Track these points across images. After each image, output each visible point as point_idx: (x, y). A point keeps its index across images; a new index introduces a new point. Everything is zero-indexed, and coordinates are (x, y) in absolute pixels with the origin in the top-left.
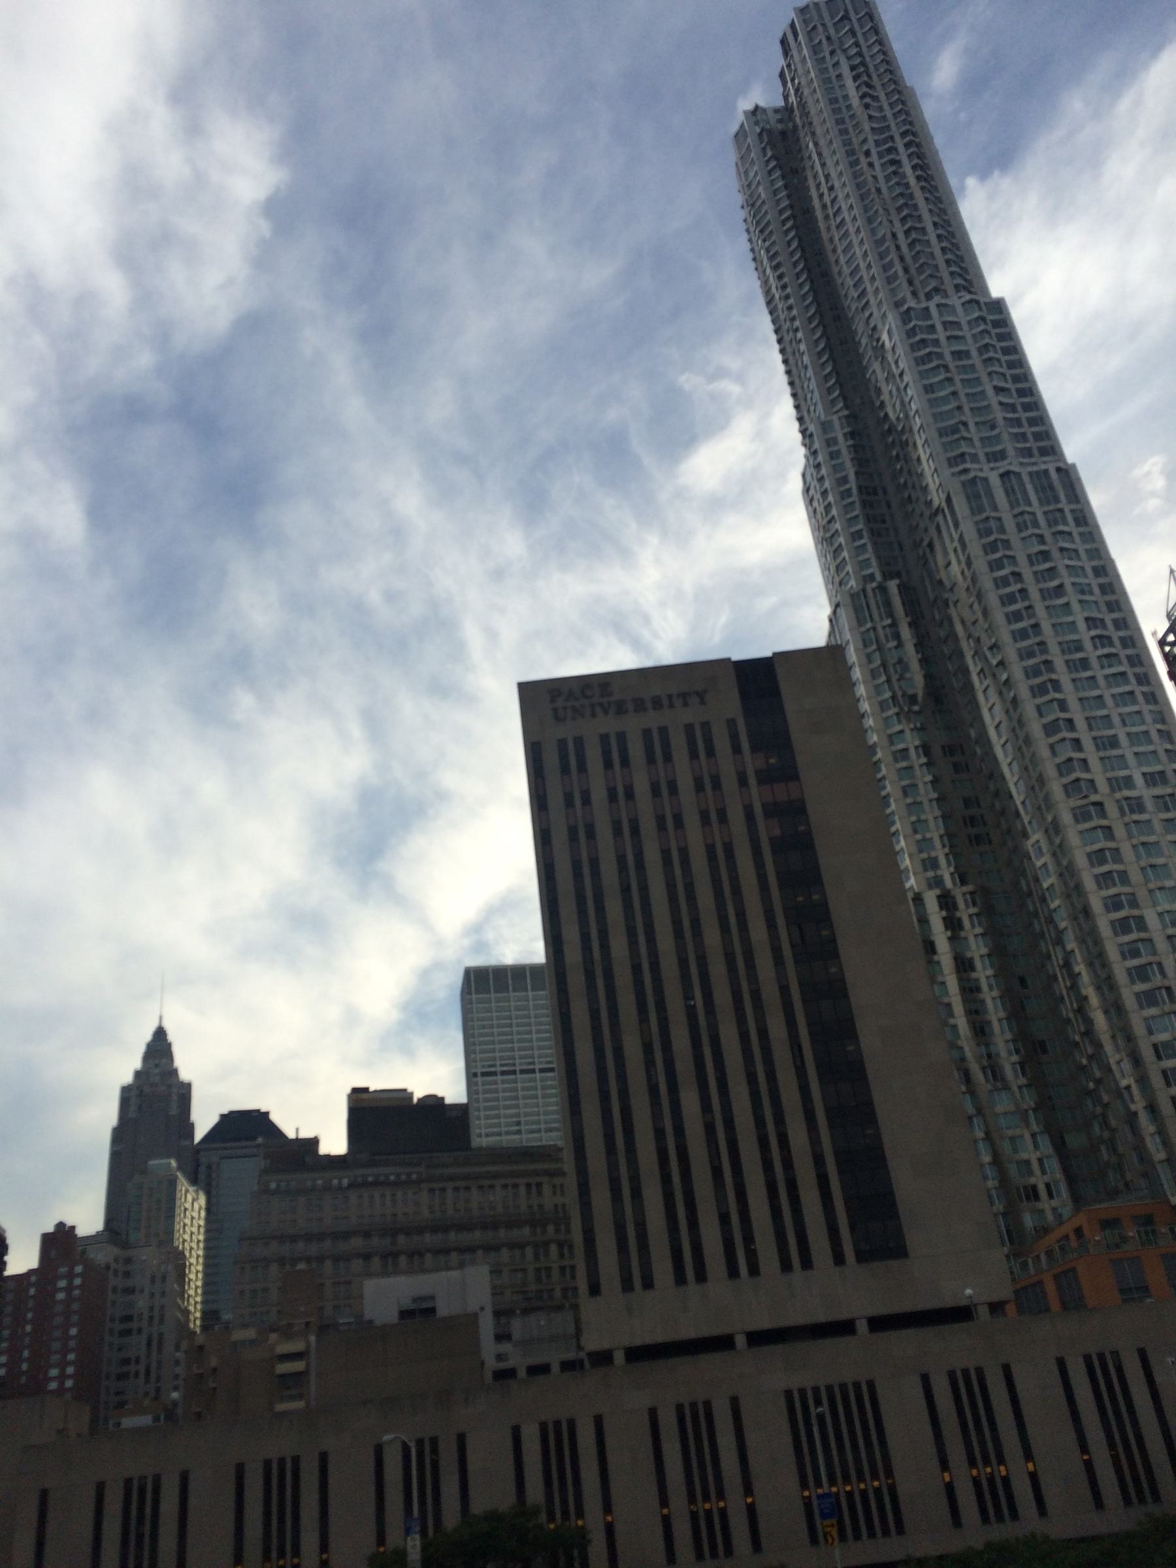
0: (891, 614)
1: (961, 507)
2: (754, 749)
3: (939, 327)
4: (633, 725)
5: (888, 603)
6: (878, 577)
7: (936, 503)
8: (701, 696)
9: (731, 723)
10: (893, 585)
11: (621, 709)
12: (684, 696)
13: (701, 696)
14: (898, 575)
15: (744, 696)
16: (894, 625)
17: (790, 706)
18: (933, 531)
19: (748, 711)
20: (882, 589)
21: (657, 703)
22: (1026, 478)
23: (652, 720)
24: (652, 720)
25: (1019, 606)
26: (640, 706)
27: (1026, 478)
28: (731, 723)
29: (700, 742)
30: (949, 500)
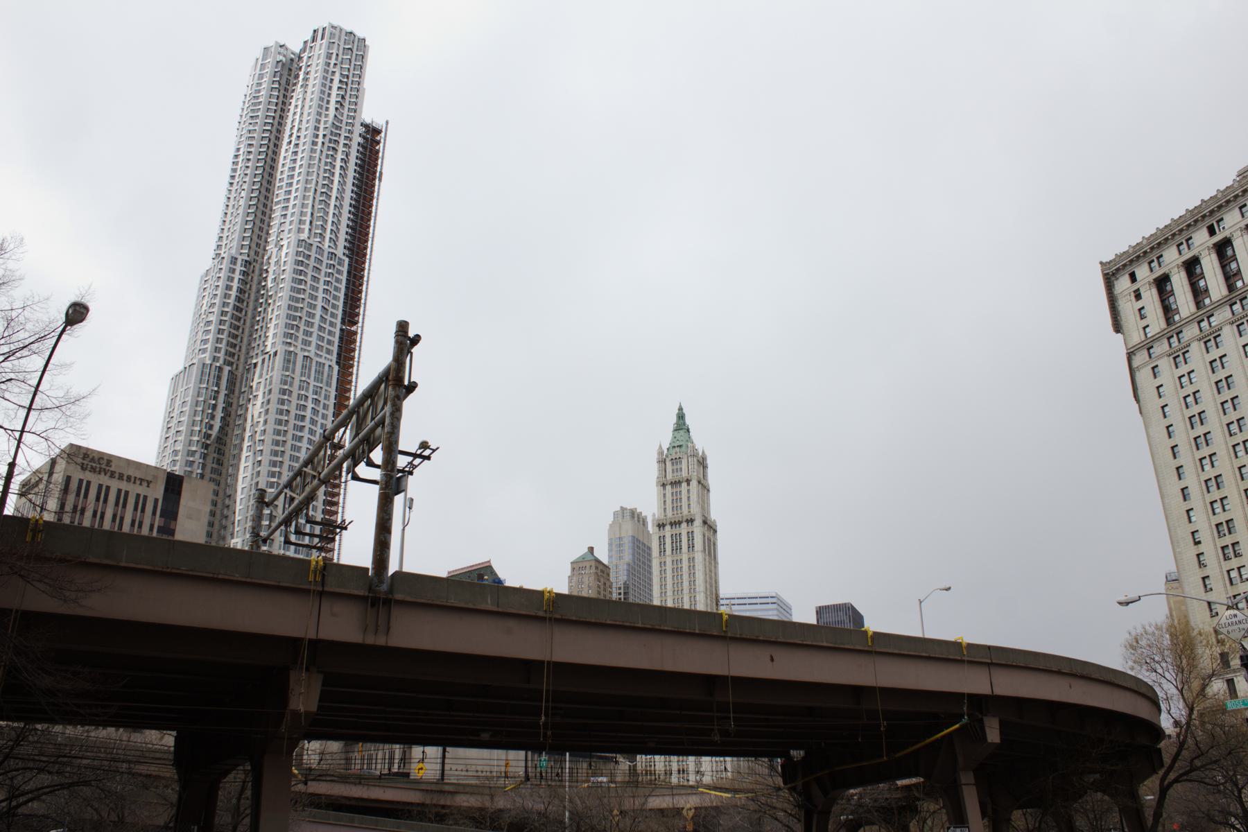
0: (218, 385)
1: (279, 360)
2: (161, 516)
3: (312, 259)
4: (115, 485)
5: (219, 378)
6: (221, 361)
7: (268, 349)
8: (149, 483)
9: (156, 500)
10: (227, 369)
11: (112, 475)
12: (141, 480)
13: (149, 483)
14: (230, 364)
15: (166, 490)
16: (217, 392)
17: (183, 501)
18: (260, 360)
19: (164, 499)
20: (220, 369)
21: (129, 478)
22: (314, 364)
23: (124, 486)
24: (124, 486)
25: (282, 428)
26: (121, 477)
27: (314, 364)
28: (156, 500)
29: (141, 502)
30: (275, 354)
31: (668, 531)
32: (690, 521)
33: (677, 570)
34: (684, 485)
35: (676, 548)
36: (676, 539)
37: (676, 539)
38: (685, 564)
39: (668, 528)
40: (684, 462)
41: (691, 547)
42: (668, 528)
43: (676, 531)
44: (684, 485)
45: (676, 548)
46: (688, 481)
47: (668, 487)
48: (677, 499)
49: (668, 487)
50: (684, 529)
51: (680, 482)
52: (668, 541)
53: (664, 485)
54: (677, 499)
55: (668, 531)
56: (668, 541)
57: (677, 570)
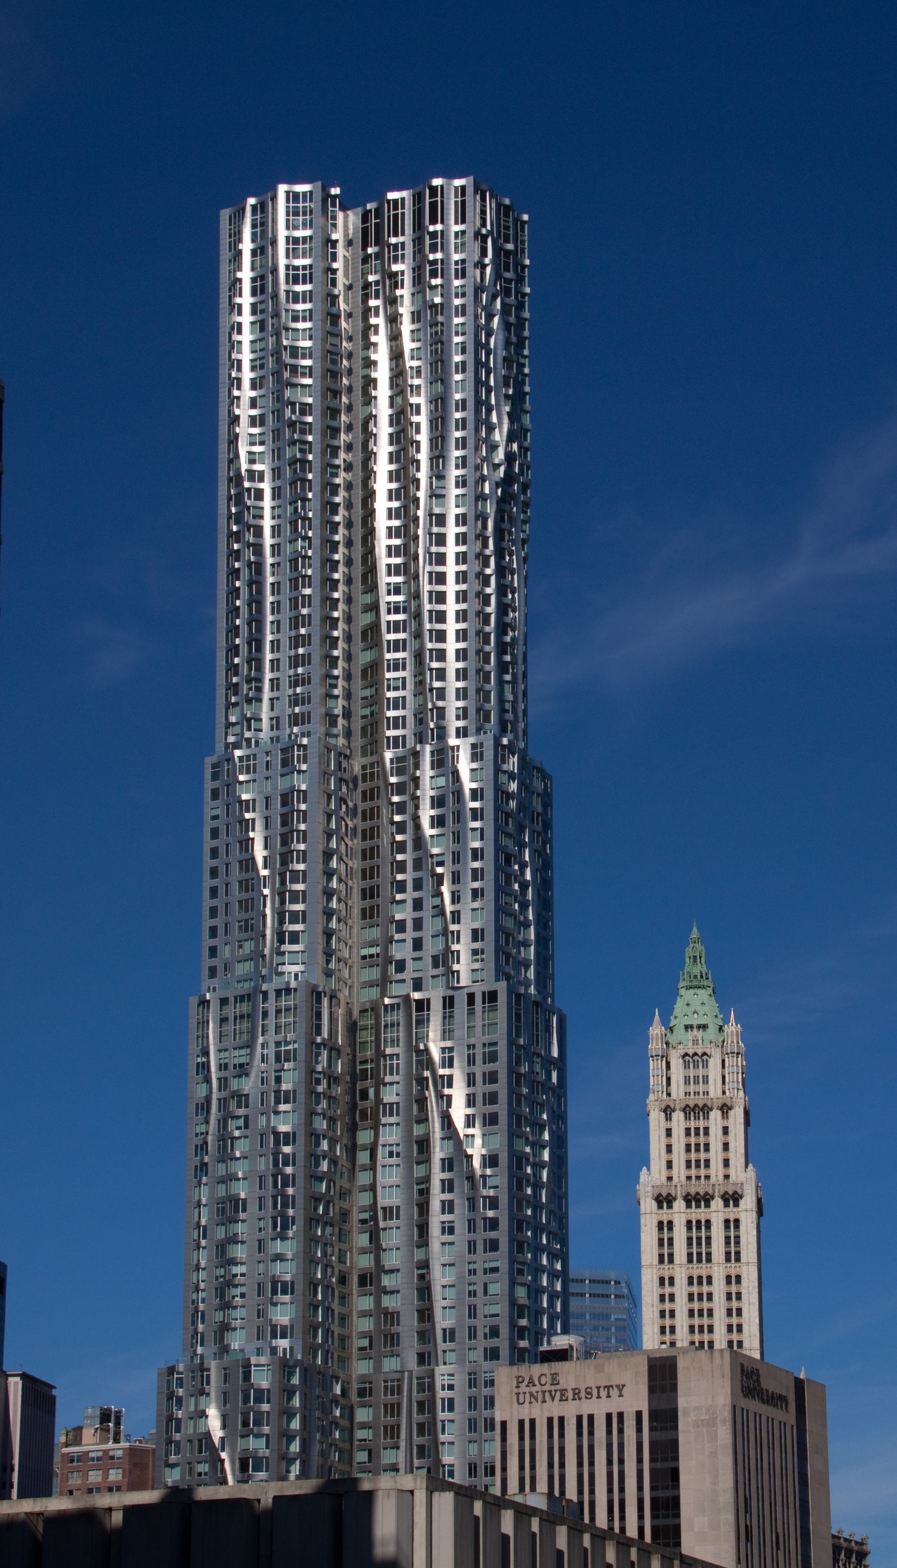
30: (491, 997)
31: (679, 1213)
32: (732, 1198)
33: (700, 1296)
34: (715, 1115)
35: (699, 1253)
36: (699, 1229)
37: (699, 1229)
38: (719, 1288)
39: (679, 1204)
40: (714, 1064)
41: (733, 1256)
42: (679, 1204)
43: (698, 1213)
44: (715, 1115)
45: (699, 1253)
46: (725, 1109)
47: (678, 1116)
48: (697, 1145)
49: (678, 1116)
50: (717, 1212)
51: (705, 1110)
52: (680, 1234)
53: (668, 1111)
54: (697, 1145)
55: (679, 1213)
56: (680, 1234)
57: (700, 1296)
